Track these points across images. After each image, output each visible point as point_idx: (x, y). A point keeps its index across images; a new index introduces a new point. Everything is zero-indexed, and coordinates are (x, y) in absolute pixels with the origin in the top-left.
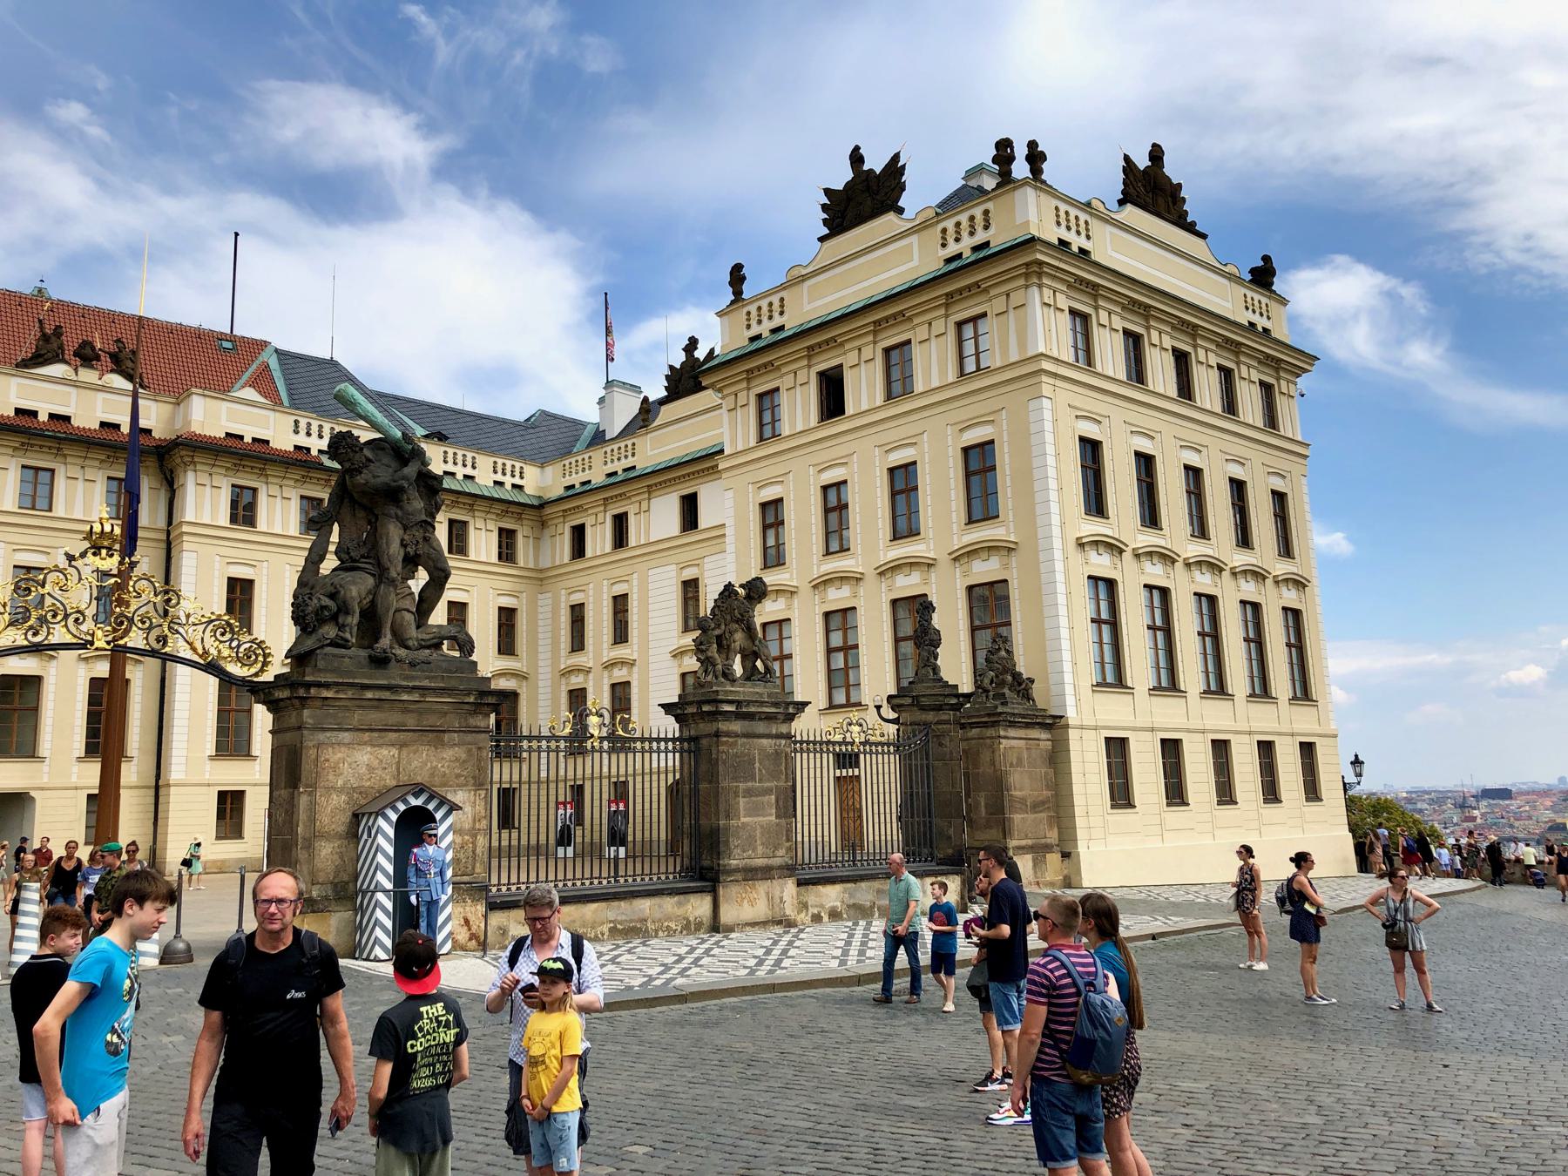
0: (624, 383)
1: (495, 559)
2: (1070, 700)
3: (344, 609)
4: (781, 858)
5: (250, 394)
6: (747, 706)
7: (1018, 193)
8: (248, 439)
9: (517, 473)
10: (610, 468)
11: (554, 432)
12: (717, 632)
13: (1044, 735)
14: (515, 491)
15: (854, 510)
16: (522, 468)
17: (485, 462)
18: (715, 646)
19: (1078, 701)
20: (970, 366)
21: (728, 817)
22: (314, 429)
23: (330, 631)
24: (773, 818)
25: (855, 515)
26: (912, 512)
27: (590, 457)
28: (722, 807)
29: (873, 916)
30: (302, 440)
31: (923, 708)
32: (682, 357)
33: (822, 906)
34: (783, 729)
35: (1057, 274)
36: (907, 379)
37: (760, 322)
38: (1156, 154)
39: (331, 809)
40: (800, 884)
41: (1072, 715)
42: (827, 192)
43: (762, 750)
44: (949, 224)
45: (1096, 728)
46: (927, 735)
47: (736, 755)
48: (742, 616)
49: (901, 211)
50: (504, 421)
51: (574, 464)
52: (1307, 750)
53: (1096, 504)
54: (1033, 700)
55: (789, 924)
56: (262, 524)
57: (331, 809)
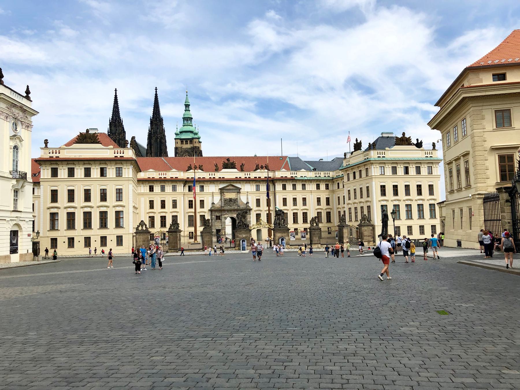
1: (325, 189)
3: (277, 223)
4: (319, 242)
5: (284, 170)
8: (284, 177)
17: (322, 173)
22: (294, 173)
23: (276, 225)
30: (292, 175)
35: (375, 163)
38: (404, 134)
39: (277, 238)
42: (354, 144)
44: (365, 154)
56: (287, 189)
57: (277, 238)
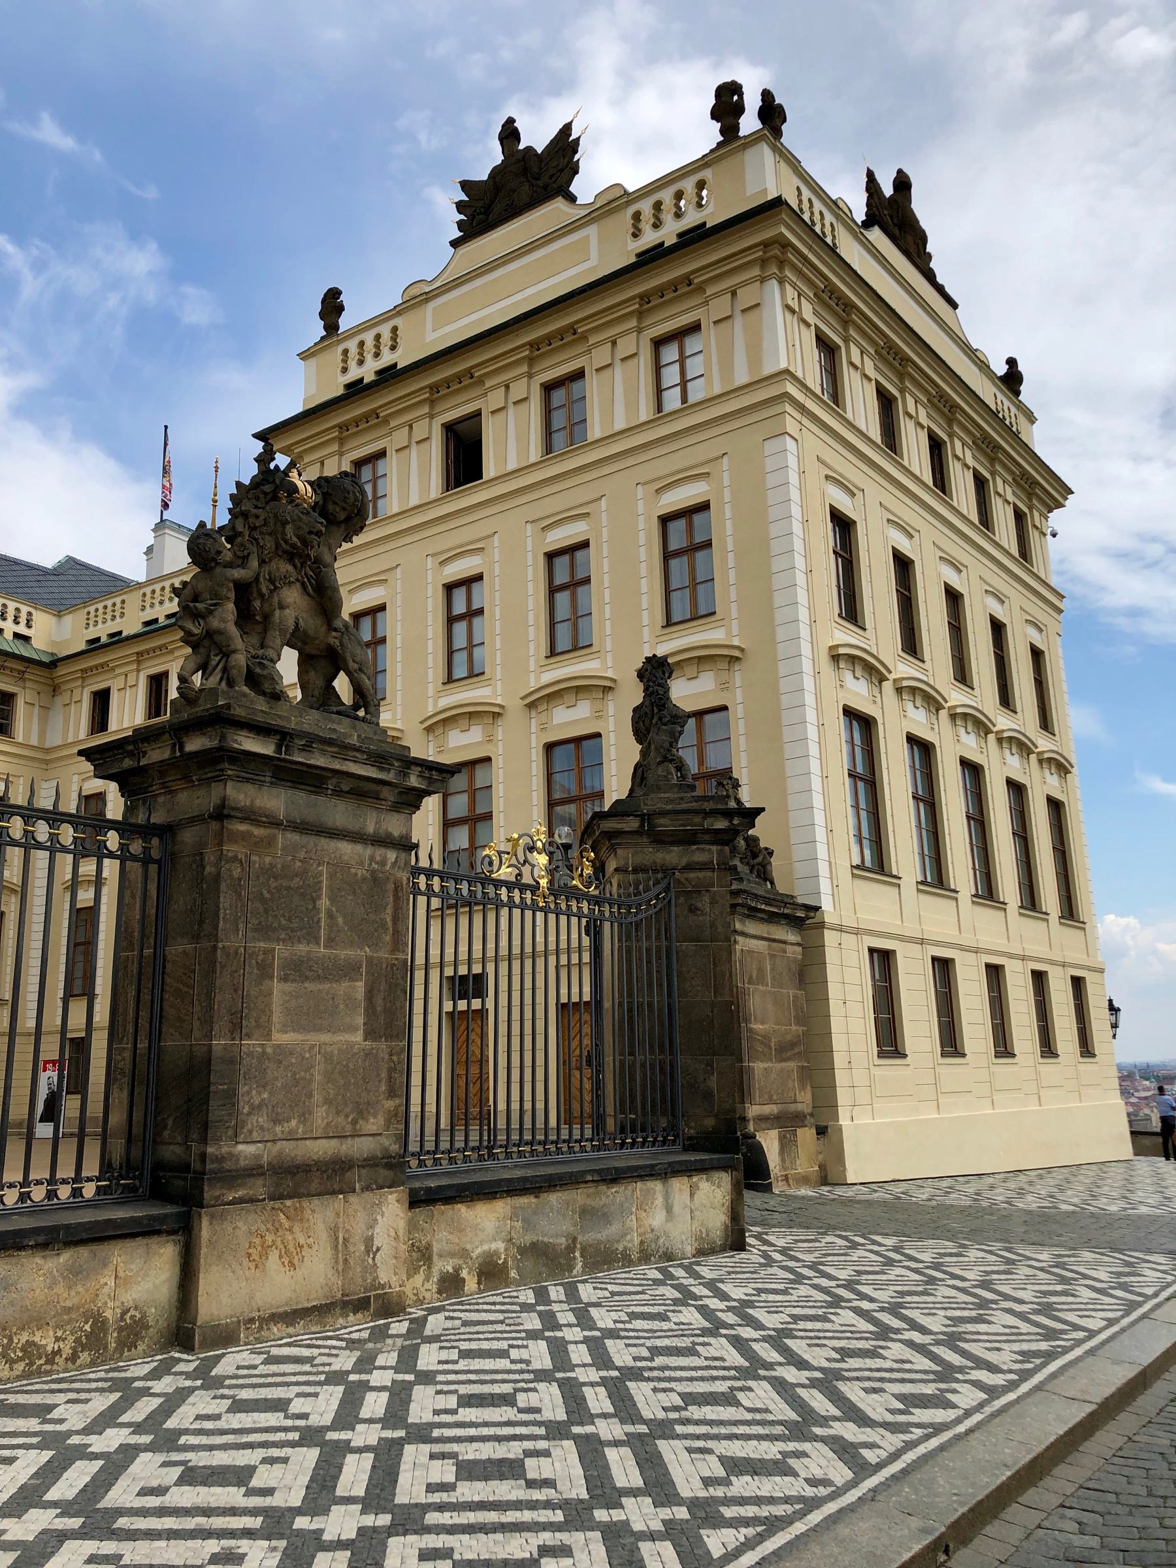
0: (179, 526)
2: (825, 886)
6: (306, 748)
7: (750, 155)
9: (23, 620)
10: (149, 615)
11: (84, 584)
12: (237, 573)
13: (792, 937)
14: (18, 642)
15: (493, 615)
16: (30, 614)
18: (231, 606)
19: (835, 886)
20: (672, 400)
21: (237, 1028)
24: (358, 1037)
25: (490, 628)
26: (579, 617)
27: (123, 602)
28: (223, 1000)
29: (571, 1268)
31: (660, 840)
32: (254, 469)
33: (464, 1254)
34: (393, 825)
36: (577, 425)
37: (361, 362)
40: (418, 1200)
41: (826, 904)
42: (466, 185)
43: (339, 867)
45: (857, 932)
46: (667, 890)
47: (269, 872)
48: (305, 543)
49: (572, 199)
50: (16, 562)
51: (101, 610)
52: (1078, 983)
53: (851, 611)
54: (772, 883)
55: (390, 1307)
